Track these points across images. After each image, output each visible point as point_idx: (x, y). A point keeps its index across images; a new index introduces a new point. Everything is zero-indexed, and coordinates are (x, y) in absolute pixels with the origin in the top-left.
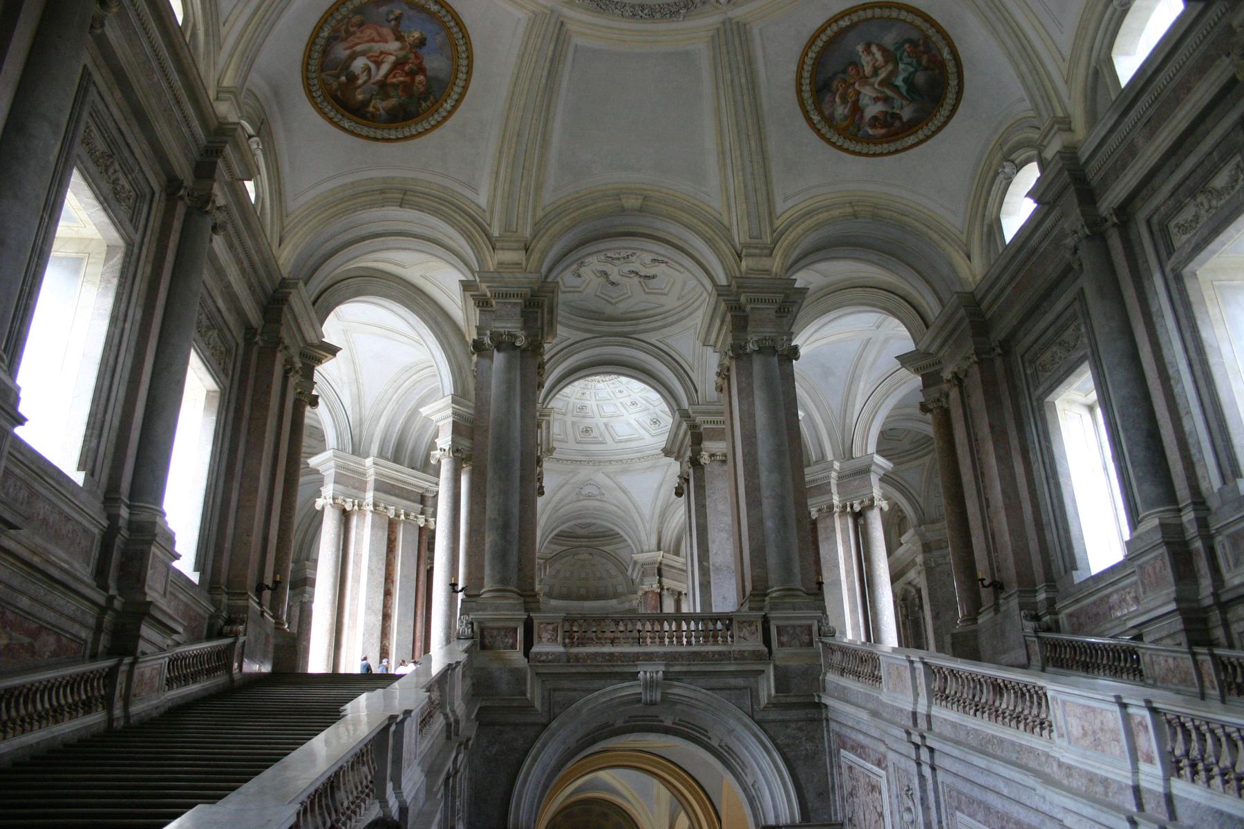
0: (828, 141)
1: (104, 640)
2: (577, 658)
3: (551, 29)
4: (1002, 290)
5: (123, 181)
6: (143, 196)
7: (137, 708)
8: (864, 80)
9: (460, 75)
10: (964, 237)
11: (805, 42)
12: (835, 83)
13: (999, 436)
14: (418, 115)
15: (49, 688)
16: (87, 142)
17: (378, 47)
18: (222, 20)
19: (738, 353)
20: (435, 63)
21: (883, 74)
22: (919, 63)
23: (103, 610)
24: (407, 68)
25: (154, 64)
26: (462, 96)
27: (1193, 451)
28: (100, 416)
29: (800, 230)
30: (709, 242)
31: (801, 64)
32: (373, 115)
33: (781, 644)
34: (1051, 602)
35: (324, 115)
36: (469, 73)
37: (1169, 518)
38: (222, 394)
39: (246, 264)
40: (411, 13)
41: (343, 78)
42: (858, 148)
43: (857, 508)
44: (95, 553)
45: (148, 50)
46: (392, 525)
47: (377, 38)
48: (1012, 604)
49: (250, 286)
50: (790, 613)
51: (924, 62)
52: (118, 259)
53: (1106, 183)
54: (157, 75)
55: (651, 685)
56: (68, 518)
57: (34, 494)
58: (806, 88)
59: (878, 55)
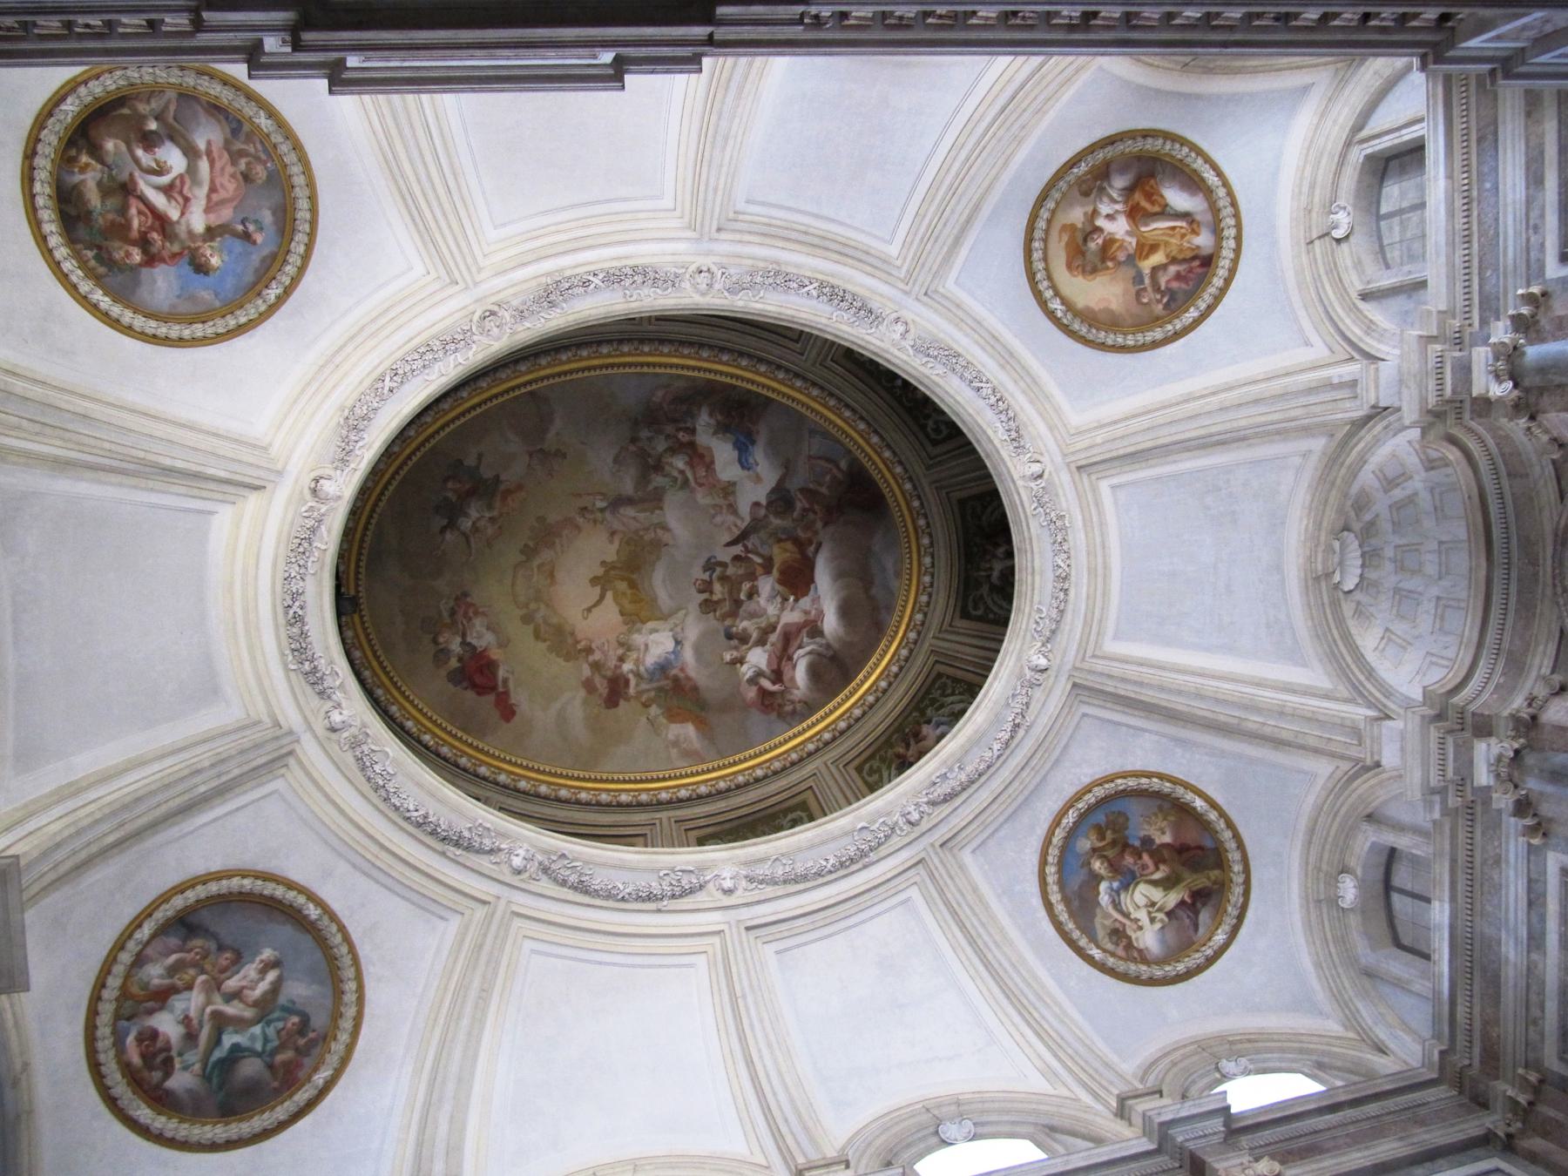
3: (250, 471)
8: (216, 985)
9: (153, 323)
11: (260, 867)
12: (197, 942)
20: (163, 284)
21: (231, 1009)
24: (155, 235)
32: (72, 161)
40: (256, 259)
41: (153, 126)
42: (104, 1030)
47: (215, 197)
51: (280, 1058)
59: (263, 986)
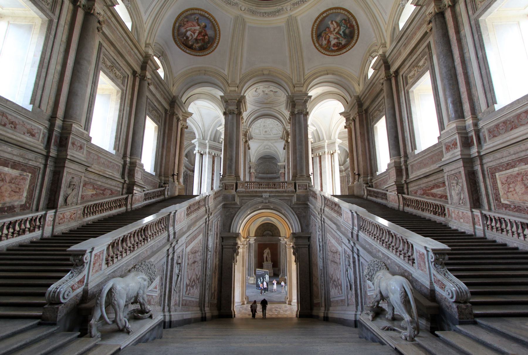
0: (321, 52)
1: (125, 191)
2: (248, 192)
4: (366, 95)
5: (118, 73)
6: (125, 77)
7: (135, 206)
10: (358, 79)
12: (322, 34)
13: (362, 135)
14: (207, 48)
15: (108, 203)
16: (104, 63)
17: (193, 28)
18: (144, 23)
19: (292, 114)
20: (210, 33)
21: (336, 30)
22: (347, 26)
23: (124, 184)
25: (122, 39)
26: (218, 42)
27: (406, 142)
28: (119, 136)
29: (311, 79)
30: (286, 83)
31: (313, 28)
33: (299, 189)
34: (371, 179)
35: (181, 49)
36: (220, 35)
37: (397, 160)
38: (159, 127)
39: (162, 93)
41: (185, 38)
43: (332, 153)
44: (121, 170)
45: (120, 35)
46: (214, 157)
48: (361, 180)
49: (164, 98)
50: (301, 181)
51: (348, 26)
52: (120, 94)
53: (393, 63)
54: (124, 42)
55: (266, 199)
56: (111, 162)
57: (99, 157)
58: (314, 36)
59: (335, 24)
